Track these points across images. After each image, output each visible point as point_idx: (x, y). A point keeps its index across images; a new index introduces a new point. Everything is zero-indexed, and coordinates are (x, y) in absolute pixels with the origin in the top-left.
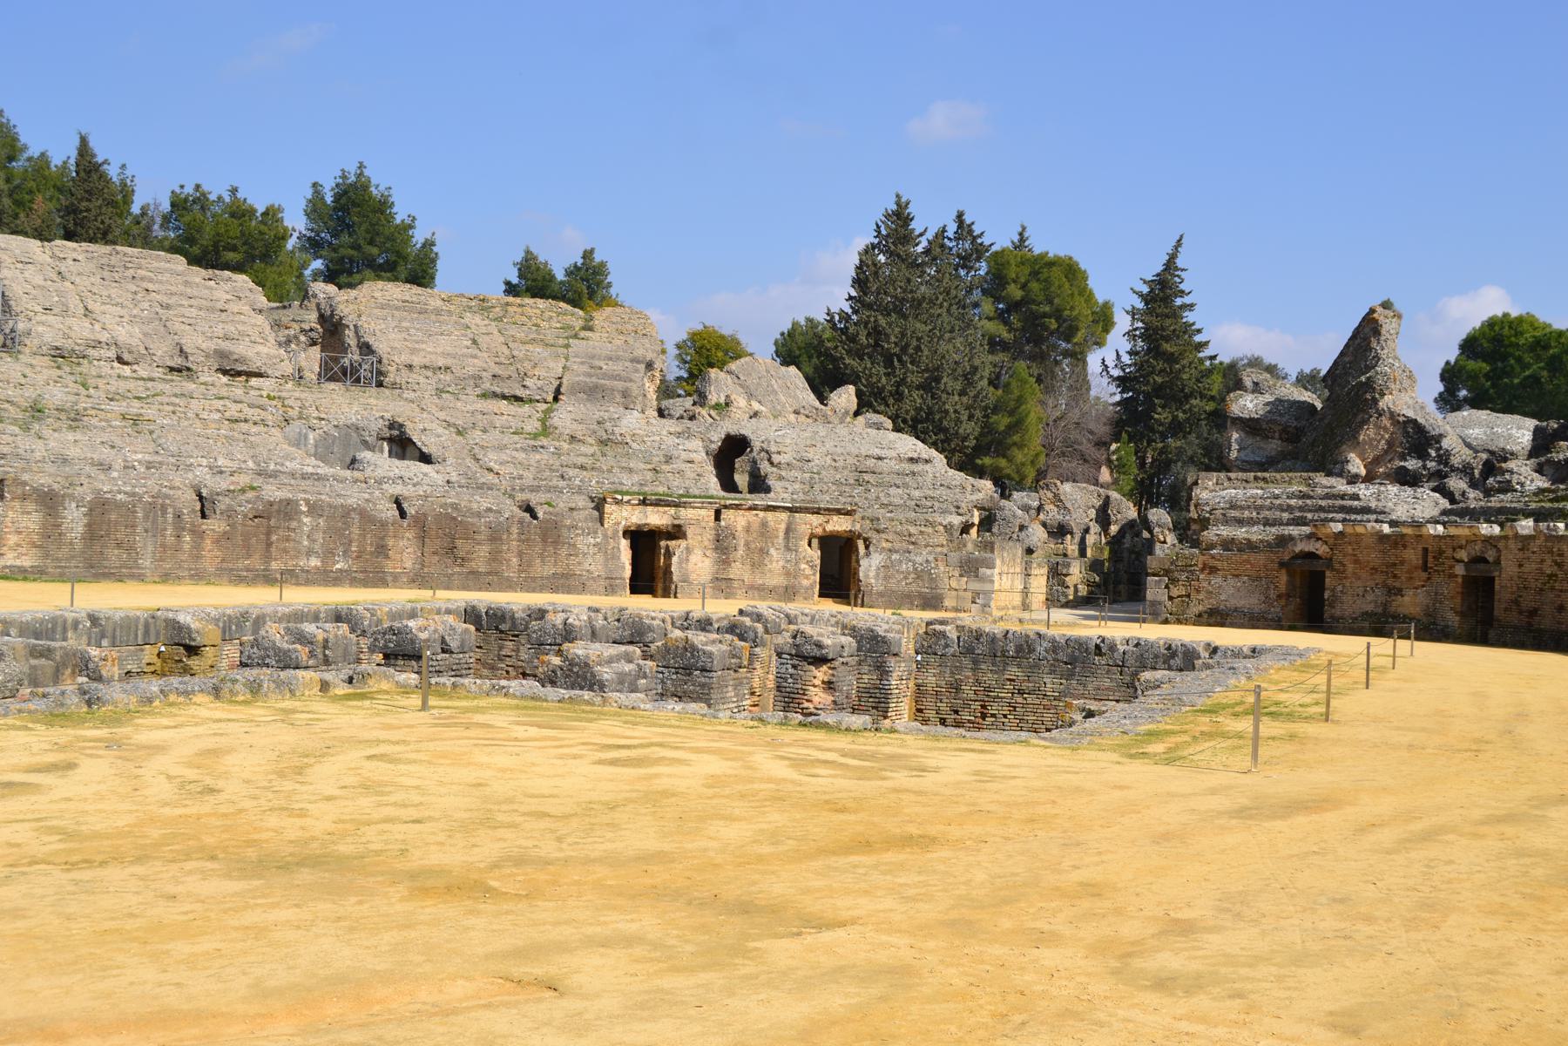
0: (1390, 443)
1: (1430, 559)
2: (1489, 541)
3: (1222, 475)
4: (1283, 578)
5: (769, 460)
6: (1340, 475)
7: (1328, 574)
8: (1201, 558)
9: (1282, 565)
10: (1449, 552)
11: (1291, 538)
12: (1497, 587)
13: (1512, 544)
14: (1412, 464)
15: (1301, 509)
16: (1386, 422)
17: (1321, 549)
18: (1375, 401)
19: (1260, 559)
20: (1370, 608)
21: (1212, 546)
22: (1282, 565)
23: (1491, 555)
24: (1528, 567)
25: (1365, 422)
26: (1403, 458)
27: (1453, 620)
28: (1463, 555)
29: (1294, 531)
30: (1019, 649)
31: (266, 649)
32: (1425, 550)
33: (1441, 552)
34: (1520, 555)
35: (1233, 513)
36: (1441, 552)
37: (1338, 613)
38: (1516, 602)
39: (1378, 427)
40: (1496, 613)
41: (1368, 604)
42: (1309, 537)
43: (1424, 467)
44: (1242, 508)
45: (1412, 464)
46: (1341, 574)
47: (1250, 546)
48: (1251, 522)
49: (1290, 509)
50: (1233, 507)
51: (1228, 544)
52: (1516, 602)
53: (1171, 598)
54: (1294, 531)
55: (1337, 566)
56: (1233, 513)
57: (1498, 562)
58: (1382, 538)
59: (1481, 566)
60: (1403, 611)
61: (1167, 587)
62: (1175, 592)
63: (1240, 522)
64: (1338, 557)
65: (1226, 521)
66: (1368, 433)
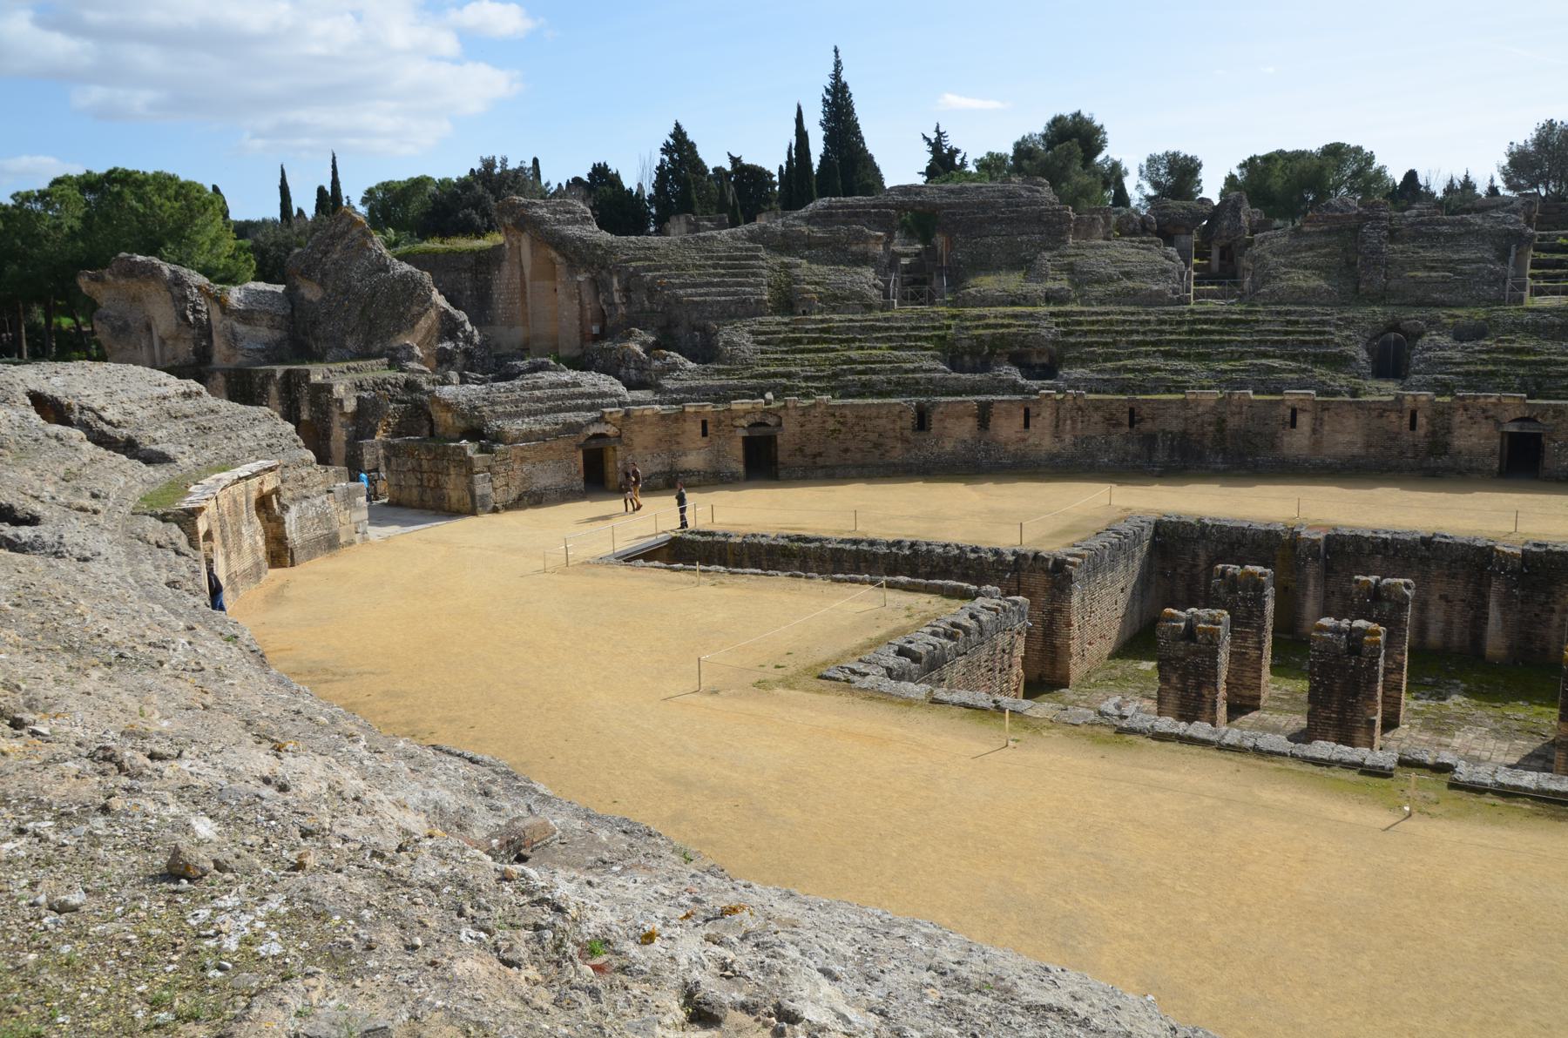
1: (710, 427)
5: (101, 418)
9: (579, 446)
10: (728, 422)
12: (779, 441)
17: (610, 430)
20: (659, 468)
21: (515, 441)
23: (771, 421)
24: (809, 427)
26: (440, 340)
27: (739, 468)
28: (744, 423)
32: (704, 423)
33: (720, 422)
34: (802, 419)
38: (801, 450)
40: (780, 459)
43: (457, 346)
46: (629, 447)
47: (543, 436)
51: (528, 436)
52: (801, 450)
53: (495, 489)
57: (780, 425)
64: (626, 433)
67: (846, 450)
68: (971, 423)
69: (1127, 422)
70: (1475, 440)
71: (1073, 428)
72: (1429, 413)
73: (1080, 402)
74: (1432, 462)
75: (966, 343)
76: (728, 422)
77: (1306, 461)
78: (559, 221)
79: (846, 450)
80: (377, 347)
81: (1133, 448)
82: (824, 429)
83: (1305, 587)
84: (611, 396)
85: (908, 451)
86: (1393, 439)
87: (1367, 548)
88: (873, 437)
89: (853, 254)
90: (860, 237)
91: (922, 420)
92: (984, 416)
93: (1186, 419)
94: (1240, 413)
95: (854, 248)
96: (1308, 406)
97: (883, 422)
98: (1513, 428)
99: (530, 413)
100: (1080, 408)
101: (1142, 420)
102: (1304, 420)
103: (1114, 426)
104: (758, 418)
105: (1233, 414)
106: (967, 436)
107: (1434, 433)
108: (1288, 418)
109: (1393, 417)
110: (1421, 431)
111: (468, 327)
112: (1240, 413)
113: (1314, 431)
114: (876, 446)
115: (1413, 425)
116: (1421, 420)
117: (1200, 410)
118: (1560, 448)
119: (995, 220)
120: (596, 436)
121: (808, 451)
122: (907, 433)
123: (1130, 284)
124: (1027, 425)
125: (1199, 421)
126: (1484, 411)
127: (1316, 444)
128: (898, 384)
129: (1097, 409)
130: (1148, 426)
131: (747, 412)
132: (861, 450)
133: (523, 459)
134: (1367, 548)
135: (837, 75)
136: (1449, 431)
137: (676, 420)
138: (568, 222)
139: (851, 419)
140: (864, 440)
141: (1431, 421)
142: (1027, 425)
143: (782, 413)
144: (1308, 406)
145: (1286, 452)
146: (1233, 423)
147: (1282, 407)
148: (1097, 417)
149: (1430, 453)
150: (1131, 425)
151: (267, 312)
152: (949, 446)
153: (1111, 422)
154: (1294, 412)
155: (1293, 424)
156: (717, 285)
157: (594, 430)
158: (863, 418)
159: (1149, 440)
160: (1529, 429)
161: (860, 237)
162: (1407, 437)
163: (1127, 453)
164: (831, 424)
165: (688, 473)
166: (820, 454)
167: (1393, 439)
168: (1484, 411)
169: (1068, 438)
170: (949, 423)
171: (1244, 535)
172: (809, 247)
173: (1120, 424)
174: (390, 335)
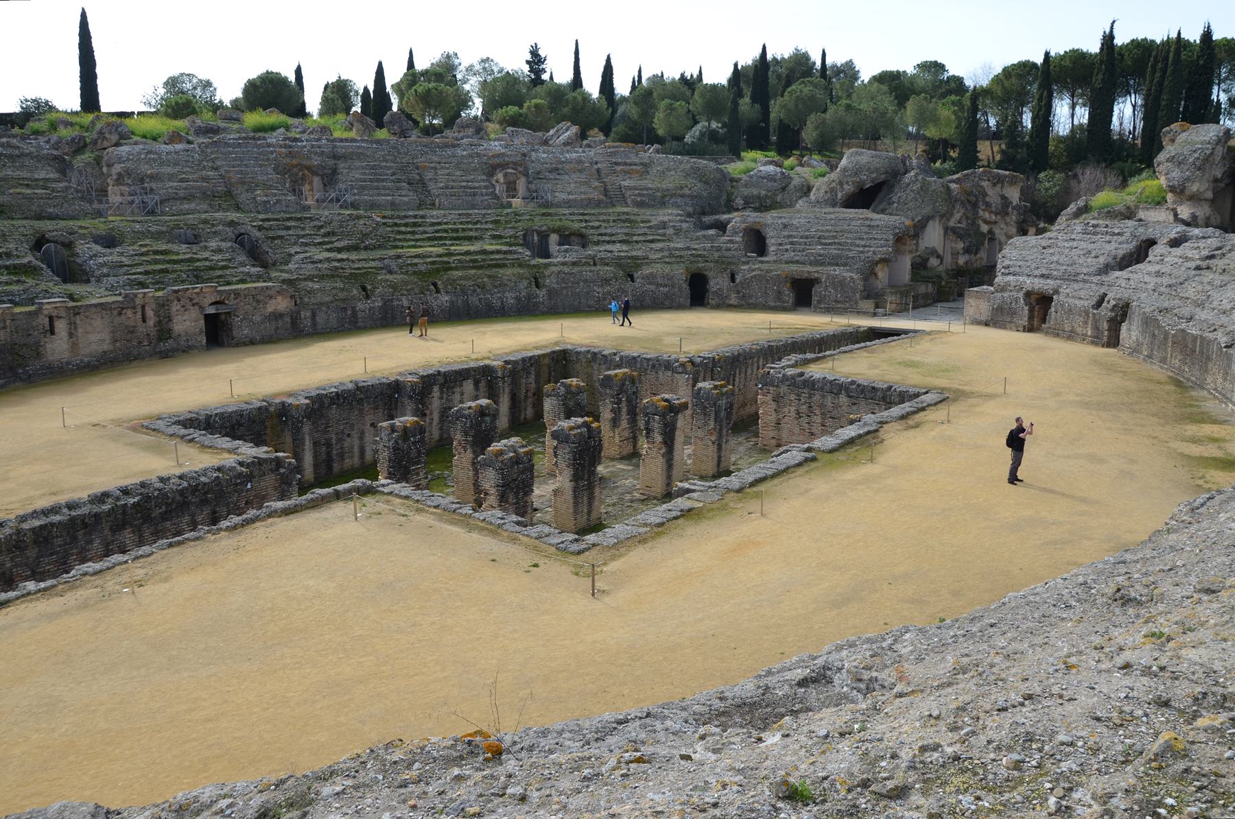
70: (188, 323)
72: (154, 306)
74: (162, 346)
77: (68, 363)
83: (303, 444)
86: (132, 332)
87: (327, 401)
96: (63, 314)
98: (211, 310)
102: (61, 326)
107: (160, 322)
108: (47, 328)
109: (129, 313)
110: (151, 323)
113: (71, 335)
115: (144, 321)
116: (150, 313)
118: (242, 321)
126: (191, 300)
127: (74, 346)
134: (327, 401)
136: (170, 319)
141: (157, 314)
144: (63, 314)
145: (51, 358)
149: (160, 339)
154: (51, 318)
155: (52, 333)
162: (142, 329)
167: (132, 332)
168: (191, 300)
171: (242, 416)
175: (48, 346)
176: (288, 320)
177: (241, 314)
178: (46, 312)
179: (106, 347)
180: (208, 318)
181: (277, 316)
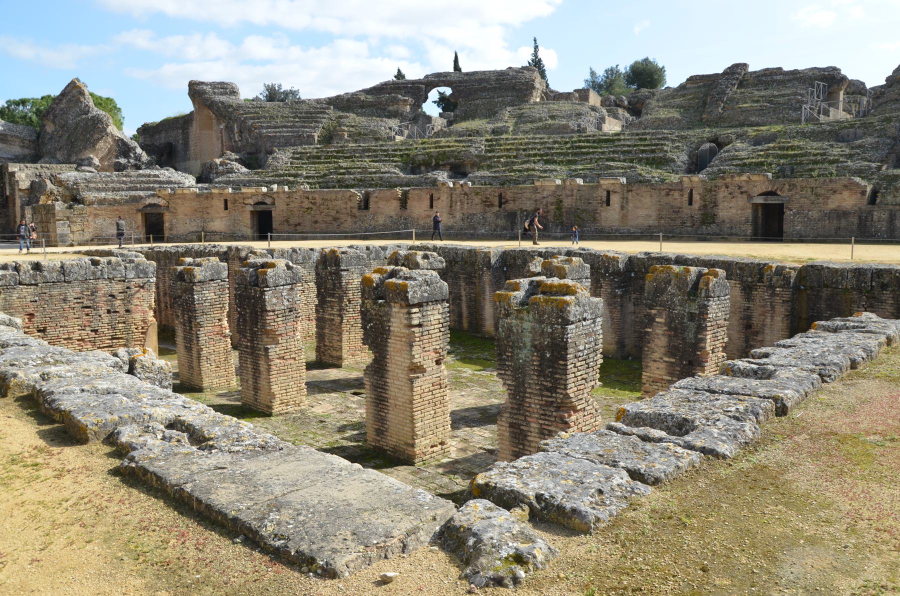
0: (110, 150)
1: (229, 204)
2: (265, 194)
3: (22, 165)
4: (139, 216)
6: (90, 165)
7: (167, 214)
8: (88, 209)
9: (139, 211)
10: (241, 201)
11: (141, 198)
12: (273, 215)
13: (282, 196)
14: (123, 161)
15: (131, 182)
16: (110, 140)
17: (162, 202)
18: (105, 129)
19: (126, 208)
20: (195, 229)
22: (139, 211)
23: (268, 201)
24: (292, 205)
25: (99, 140)
26: (117, 157)
27: (249, 232)
28: (251, 201)
29: (141, 193)
30: (304, 258)
31: (584, 305)
32: (226, 201)
33: (235, 201)
34: (288, 200)
35: (92, 185)
36: (235, 201)
37: (174, 232)
38: (287, 221)
39: (105, 142)
40: (274, 227)
41: (192, 226)
42: (153, 195)
43: (129, 162)
44: (95, 182)
45: (123, 161)
46: (174, 214)
47: (114, 202)
48: (104, 190)
49: (124, 182)
50: (89, 181)
51: (101, 202)
52: (287, 221)
54: (141, 193)
55: (172, 210)
56: (92, 185)
57: (273, 204)
58: (198, 196)
59: (264, 206)
60: (213, 229)
61: (69, 226)
62: (75, 228)
63: (99, 190)
64: (172, 205)
65: (90, 190)
66: (101, 144)
67: (316, 222)
68: (395, 204)
69: (497, 203)
70: (734, 211)
71: (462, 208)
72: (701, 191)
73: (466, 190)
75: (421, 158)
76: (241, 201)
77: (617, 231)
78: (215, 93)
79: (316, 222)
80: (74, 158)
81: (501, 222)
82: (302, 207)
83: (484, 292)
84: (175, 183)
85: (355, 223)
86: (677, 212)
88: (333, 213)
89: (389, 112)
90: (395, 101)
91: (365, 204)
92: (404, 202)
93: (536, 201)
94: (572, 195)
95: (391, 108)
96: (619, 190)
97: (339, 203)
98: (760, 200)
99: (114, 190)
100: (466, 194)
101: (506, 202)
102: (615, 199)
103: (489, 206)
104: (260, 199)
105: (567, 196)
106: (393, 214)
107: (705, 206)
108: (604, 199)
109: (676, 194)
110: (696, 205)
111: (139, 150)
112: (572, 195)
113: (622, 208)
114: (335, 219)
115: (690, 203)
116: (696, 197)
117: (545, 193)
118: (794, 215)
119: (485, 89)
120: (150, 205)
121: (292, 222)
122: (355, 211)
123: (557, 122)
124: (432, 206)
125: (544, 201)
126: (740, 187)
127: (624, 217)
128: (361, 180)
129: (477, 194)
130: (510, 206)
131: (253, 195)
132: (326, 222)
133: (96, 216)
135: (535, 54)
136: (716, 205)
137: (207, 198)
138: (221, 94)
139: (319, 201)
140: (327, 215)
141: (703, 198)
142: (432, 206)
143: (274, 196)
144: (619, 190)
145: (604, 224)
146: (567, 202)
147: (600, 190)
148: (477, 200)
149: (703, 222)
150: (500, 206)
151: (17, 137)
152: (381, 220)
153: (487, 203)
154: (608, 192)
155: (608, 204)
156: (290, 127)
157: (149, 201)
158: (326, 200)
159: (512, 217)
160: (772, 200)
161: (395, 101)
162: (687, 211)
163: (497, 226)
164: (306, 204)
165: (214, 233)
166: (299, 224)
167: (677, 212)
168: (740, 187)
169: (458, 215)
170: (381, 204)
171: (457, 253)
172: (362, 107)
173: (492, 205)
174: (80, 151)
175: (603, 214)
176: (855, 220)
177: (795, 207)
178: (605, 187)
179: (651, 222)
180: (756, 206)
181: (841, 214)
